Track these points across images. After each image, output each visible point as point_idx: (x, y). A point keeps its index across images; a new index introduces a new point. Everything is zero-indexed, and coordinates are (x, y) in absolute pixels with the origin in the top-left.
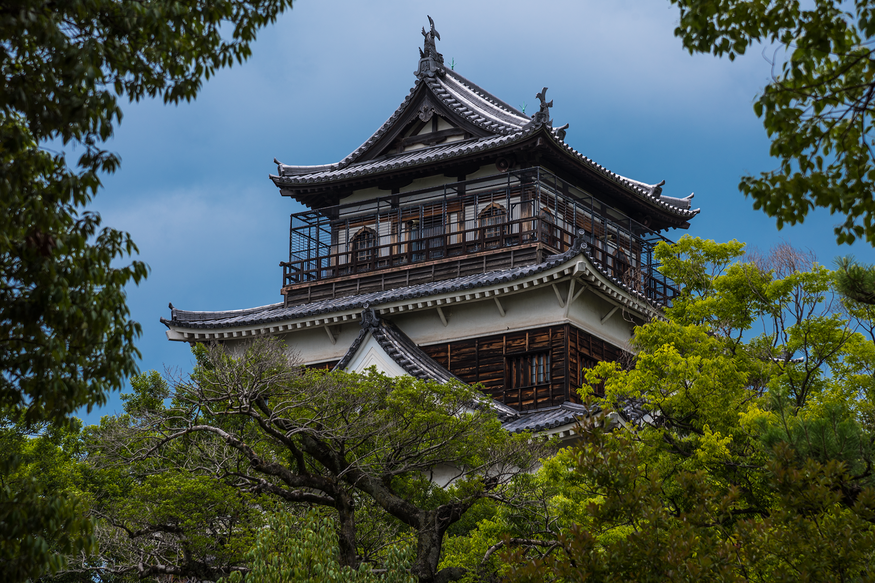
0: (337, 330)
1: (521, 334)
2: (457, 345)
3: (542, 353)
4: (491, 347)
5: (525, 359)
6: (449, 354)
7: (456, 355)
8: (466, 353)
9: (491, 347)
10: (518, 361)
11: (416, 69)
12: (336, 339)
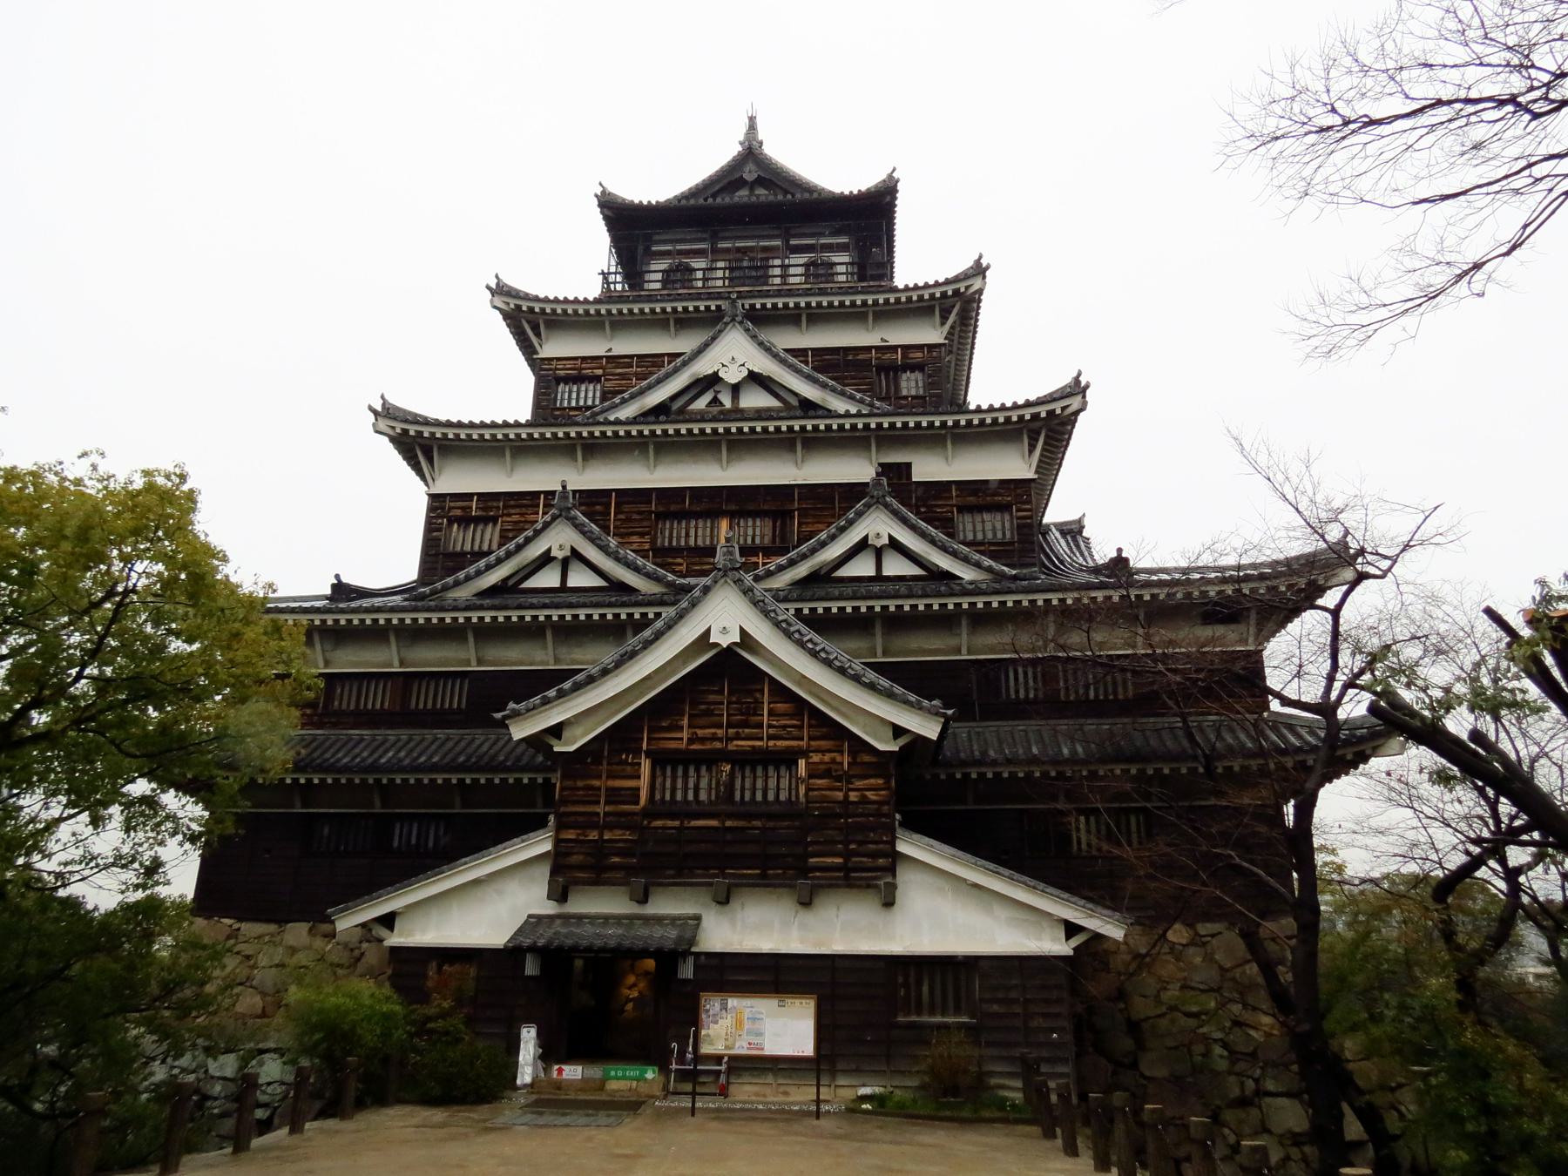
0: (684, 322)
8: (825, 360)
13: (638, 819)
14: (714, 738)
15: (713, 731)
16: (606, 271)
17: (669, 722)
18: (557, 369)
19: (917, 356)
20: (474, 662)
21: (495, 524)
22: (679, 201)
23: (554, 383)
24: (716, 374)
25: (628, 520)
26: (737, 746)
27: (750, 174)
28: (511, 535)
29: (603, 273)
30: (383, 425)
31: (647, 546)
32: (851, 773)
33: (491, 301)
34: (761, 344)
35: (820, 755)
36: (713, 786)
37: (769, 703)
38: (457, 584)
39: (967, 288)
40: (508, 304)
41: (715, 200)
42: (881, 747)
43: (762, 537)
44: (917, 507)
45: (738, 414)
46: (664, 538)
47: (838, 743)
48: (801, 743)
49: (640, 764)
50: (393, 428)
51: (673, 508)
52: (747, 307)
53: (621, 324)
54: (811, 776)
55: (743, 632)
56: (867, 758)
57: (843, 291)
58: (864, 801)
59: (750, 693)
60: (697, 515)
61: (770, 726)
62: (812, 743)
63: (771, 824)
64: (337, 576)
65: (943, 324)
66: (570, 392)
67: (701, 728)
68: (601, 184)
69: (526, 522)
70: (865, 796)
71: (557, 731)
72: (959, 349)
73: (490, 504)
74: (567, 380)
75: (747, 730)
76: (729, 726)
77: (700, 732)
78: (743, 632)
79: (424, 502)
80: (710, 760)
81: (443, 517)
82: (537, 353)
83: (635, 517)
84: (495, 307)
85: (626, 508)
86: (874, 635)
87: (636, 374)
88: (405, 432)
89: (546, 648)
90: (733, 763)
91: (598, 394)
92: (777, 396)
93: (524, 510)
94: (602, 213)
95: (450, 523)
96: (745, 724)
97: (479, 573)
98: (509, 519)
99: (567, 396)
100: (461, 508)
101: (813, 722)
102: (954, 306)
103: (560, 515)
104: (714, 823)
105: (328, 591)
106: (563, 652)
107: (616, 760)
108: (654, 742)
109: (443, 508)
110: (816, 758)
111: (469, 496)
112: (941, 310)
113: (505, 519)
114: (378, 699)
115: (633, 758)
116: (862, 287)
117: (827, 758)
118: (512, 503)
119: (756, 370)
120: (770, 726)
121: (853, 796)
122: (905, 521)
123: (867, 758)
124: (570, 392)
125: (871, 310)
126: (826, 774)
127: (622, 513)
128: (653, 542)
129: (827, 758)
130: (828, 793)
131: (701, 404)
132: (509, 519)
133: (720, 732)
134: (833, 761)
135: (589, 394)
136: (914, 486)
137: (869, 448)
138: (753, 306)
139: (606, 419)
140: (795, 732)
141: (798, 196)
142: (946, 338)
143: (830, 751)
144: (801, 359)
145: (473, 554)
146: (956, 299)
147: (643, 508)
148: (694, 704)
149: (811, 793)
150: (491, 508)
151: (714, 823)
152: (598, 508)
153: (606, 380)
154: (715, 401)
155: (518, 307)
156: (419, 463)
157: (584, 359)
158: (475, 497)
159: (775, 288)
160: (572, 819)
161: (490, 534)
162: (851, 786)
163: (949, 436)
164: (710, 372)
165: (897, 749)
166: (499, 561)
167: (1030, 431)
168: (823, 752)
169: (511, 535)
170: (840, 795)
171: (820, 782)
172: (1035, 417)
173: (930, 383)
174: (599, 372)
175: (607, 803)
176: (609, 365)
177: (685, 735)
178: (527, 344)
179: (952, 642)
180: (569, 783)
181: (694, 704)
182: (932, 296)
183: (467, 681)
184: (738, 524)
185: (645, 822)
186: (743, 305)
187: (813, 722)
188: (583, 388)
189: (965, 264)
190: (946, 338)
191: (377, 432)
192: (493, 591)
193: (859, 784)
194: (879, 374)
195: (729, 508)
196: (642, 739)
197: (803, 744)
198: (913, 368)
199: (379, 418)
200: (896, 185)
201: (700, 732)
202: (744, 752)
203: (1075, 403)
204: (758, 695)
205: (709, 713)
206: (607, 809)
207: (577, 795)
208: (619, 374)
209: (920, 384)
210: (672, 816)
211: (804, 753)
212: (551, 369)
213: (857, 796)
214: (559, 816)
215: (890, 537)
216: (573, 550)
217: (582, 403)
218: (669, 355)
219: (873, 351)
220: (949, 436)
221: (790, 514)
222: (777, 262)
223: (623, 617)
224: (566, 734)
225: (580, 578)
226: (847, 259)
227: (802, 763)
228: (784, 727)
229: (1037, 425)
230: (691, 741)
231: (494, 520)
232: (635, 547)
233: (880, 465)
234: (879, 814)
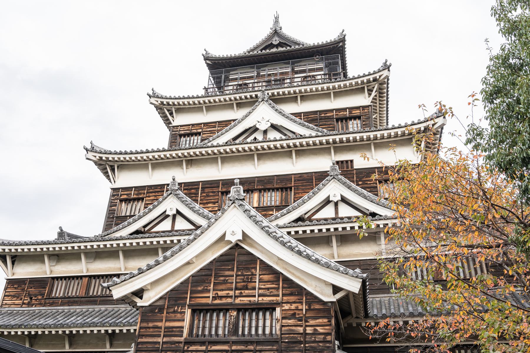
0: (240, 105)
1: (344, 109)
2: (306, 114)
3: (359, 118)
4: (326, 115)
5: (346, 121)
6: (302, 117)
7: (306, 118)
9: (326, 115)
10: (342, 121)
13: (182, 345)
14: (227, 297)
15: (227, 292)
16: (207, 87)
17: (202, 287)
18: (180, 131)
19: (356, 112)
20: (123, 269)
21: (142, 201)
23: (178, 137)
24: (255, 126)
25: (208, 196)
26: (241, 300)
27: (276, 41)
29: (205, 88)
30: (90, 155)
32: (307, 316)
33: (149, 100)
34: (276, 110)
35: (289, 305)
36: (227, 325)
37: (260, 275)
39: (380, 77)
40: (157, 101)
42: (325, 299)
43: (275, 202)
44: (357, 181)
47: (299, 297)
48: (278, 298)
49: (184, 312)
50: (95, 157)
52: (270, 94)
53: (211, 108)
54: (283, 318)
55: (244, 234)
56: (317, 307)
58: (316, 333)
59: (248, 269)
61: (259, 289)
62: (285, 298)
63: (258, 348)
64: (60, 228)
66: (186, 141)
67: (223, 290)
68: (205, 50)
70: (315, 330)
71: (139, 293)
72: (380, 111)
73: (140, 192)
74: (184, 135)
75: (247, 291)
76: (236, 289)
78: (244, 234)
79: (109, 192)
80: (224, 309)
81: (117, 199)
82: (170, 123)
83: (211, 194)
84: (151, 103)
85: (207, 190)
86: (333, 246)
88: (101, 158)
90: (239, 310)
93: (157, 194)
94: (206, 63)
95: (121, 201)
98: (149, 199)
101: (286, 286)
102: (374, 88)
104: (226, 347)
105: (56, 236)
107: (172, 310)
108: (193, 299)
109: (118, 195)
110: (286, 307)
111: (129, 189)
112: (368, 90)
113: (147, 198)
114: (75, 290)
115: (181, 309)
117: (293, 307)
118: (151, 191)
119: (275, 123)
120: (259, 289)
121: (309, 330)
122: (349, 187)
123: (317, 307)
124: (186, 141)
126: (293, 316)
127: (204, 193)
129: (293, 307)
130: (294, 328)
132: (149, 199)
133: (231, 293)
134: (297, 309)
136: (355, 171)
138: (273, 94)
140: (275, 292)
143: (294, 302)
144: (299, 117)
146: (376, 82)
147: (215, 190)
148: (217, 276)
149: (283, 329)
150: (141, 194)
151: (226, 347)
152: (193, 191)
153: (203, 134)
155: (162, 103)
156: (107, 172)
157: (193, 125)
158: (134, 189)
160: (145, 346)
162: (307, 324)
163: (372, 144)
164: (252, 125)
165: (335, 300)
168: (291, 303)
170: (301, 330)
171: (290, 321)
173: (364, 125)
174: (200, 130)
175: (165, 336)
176: (205, 127)
177: (211, 295)
178: (168, 122)
180: (144, 325)
181: (217, 276)
182: (363, 82)
184: (263, 196)
185: (186, 348)
186: (268, 94)
187: (286, 286)
188: (192, 138)
189: (378, 66)
191: (87, 159)
192: (137, 232)
193: (312, 322)
195: (258, 187)
197: (279, 299)
198: (355, 118)
200: (344, 37)
201: (220, 293)
202: (245, 304)
204: (253, 271)
205: (225, 282)
206: (164, 340)
207: (149, 331)
208: (209, 131)
209: (359, 125)
210: (202, 343)
211: (278, 304)
212: (177, 131)
213: (311, 330)
214: (137, 344)
215: (341, 196)
219: (334, 111)
220: (372, 144)
221: (291, 188)
224: (146, 296)
227: (278, 310)
228: (268, 289)
230: (214, 298)
231: (142, 199)
232: (210, 209)
234: (324, 341)
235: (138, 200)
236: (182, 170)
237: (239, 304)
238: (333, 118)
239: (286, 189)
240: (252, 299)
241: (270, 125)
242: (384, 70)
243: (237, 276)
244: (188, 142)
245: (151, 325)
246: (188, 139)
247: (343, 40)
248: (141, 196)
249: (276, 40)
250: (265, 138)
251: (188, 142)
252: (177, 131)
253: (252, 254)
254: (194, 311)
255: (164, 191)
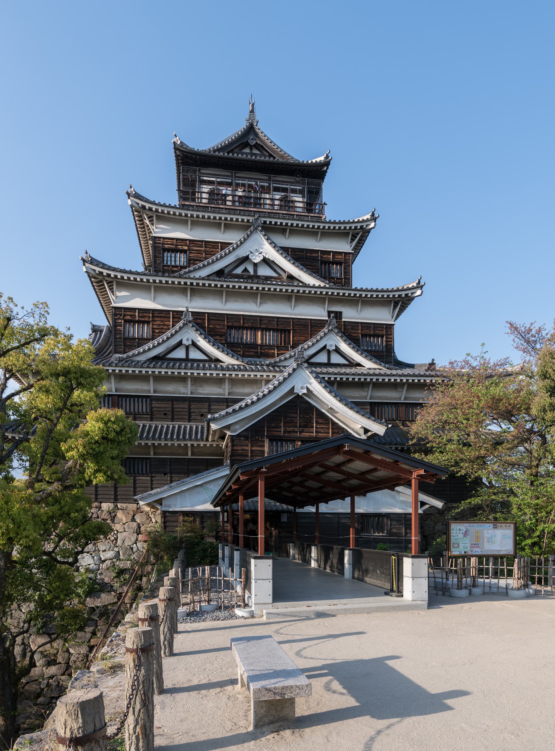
1: (328, 253)
5: (329, 265)
10: (325, 265)
11: (247, 117)
12: (224, 232)
14: (294, 432)
18: (163, 244)
22: (215, 151)
28: (157, 331)
31: (224, 342)
38: (139, 354)
39: (367, 226)
41: (233, 155)
45: (256, 278)
46: (231, 338)
49: (264, 441)
51: (236, 324)
57: (300, 217)
60: (247, 328)
65: (351, 242)
66: (171, 257)
69: (164, 325)
73: (145, 314)
74: (169, 250)
77: (288, 429)
81: (121, 319)
85: (213, 322)
87: (205, 251)
89: (187, 387)
91: (185, 260)
92: (275, 271)
94: (175, 153)
95: (126, 321)
96: (306, 426)
97: (149, 349)
99: (170, 259)
100: (131, 316)
102: (358, 234)
103: (187, 324)
106: (194, 388)
107: (254, 439)
111: (134, 310)
112: (352, 235)
115: (261, 438)
116: (311, 216)
119: (267, 257)
125: (320, 231)
128: (226, 340)
131: (239, 271)
133: (296, 429)
135: (181, 259)
137: (324, 303)
139: (194, 276)
141: (277, 158)
142: (352, 250)
145: (139, 339)
147: (221, 323)
154: (246, 270)
157: (177, 239)
159: (269, 211)
161: (146, 331)
164: (245, 255)
165: (366, 438)
166: (159, 344)
167: (395, 302)
169: (157, 331)
172: (400, 296)
174: (186, 248)
179: (364, 394)
183: (148, 400)
188: (178, 255)
190: (352, 250)
192: (156, 358)
194: (321, 264)
196: (264, 431)
198: (338, 263)
199: (86, 264)
201: (288, 429)
203: (419, 292)
204: (311, 415)
208: (196, 250)
212: (160, 244)
215: (336, 346)
216: (193, 341)
217: (178, 263)
218: (221, 243)
221: (289, 331)
222: (267, 196)
223: (227, 376)
224: (232, 428)
225: (195, 354)
226: (301, 199)
229: (399, 299)
231: (148, 323)
233: (329, 313)
235: (143, 322)
236: (185, 297)
237: (303, 437)
238: (318, 260)
239: (285, 331)
240: (311, 434)
241: (262, 258)
242: (371, 220)
243: (300, 417)
244: (173, 259)
245: (239, 448)
246: (173, 255)
247: (327, 164)
248: (146, 319)
249: (252, 139)
250: (255, 271)
251: (173, 259)
252: (160, 244)
253: (309, 403)
254: (270, 440)
255: (170, 317)
